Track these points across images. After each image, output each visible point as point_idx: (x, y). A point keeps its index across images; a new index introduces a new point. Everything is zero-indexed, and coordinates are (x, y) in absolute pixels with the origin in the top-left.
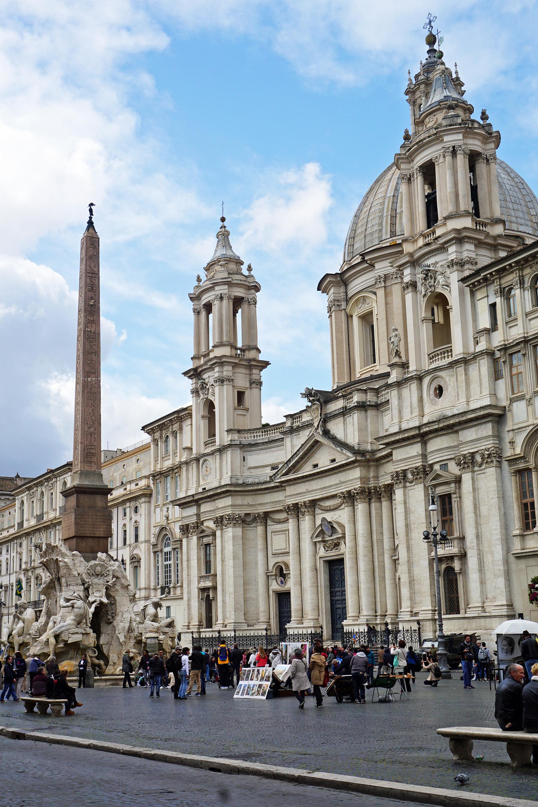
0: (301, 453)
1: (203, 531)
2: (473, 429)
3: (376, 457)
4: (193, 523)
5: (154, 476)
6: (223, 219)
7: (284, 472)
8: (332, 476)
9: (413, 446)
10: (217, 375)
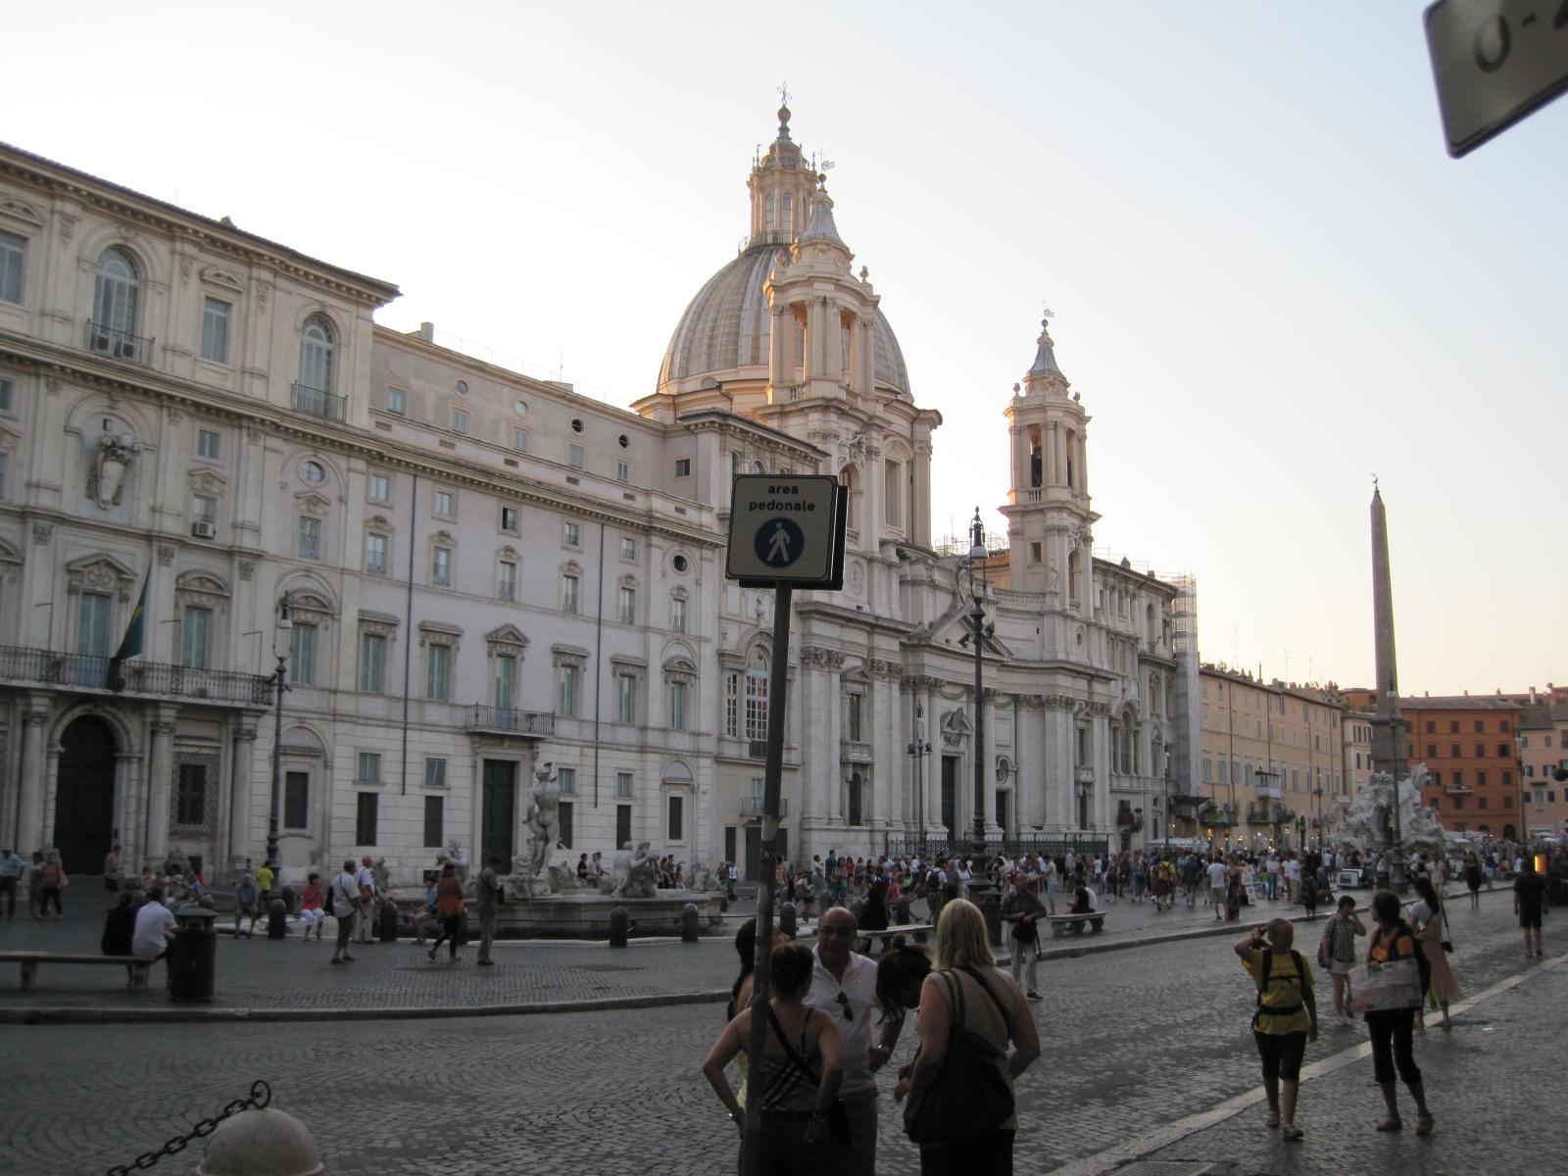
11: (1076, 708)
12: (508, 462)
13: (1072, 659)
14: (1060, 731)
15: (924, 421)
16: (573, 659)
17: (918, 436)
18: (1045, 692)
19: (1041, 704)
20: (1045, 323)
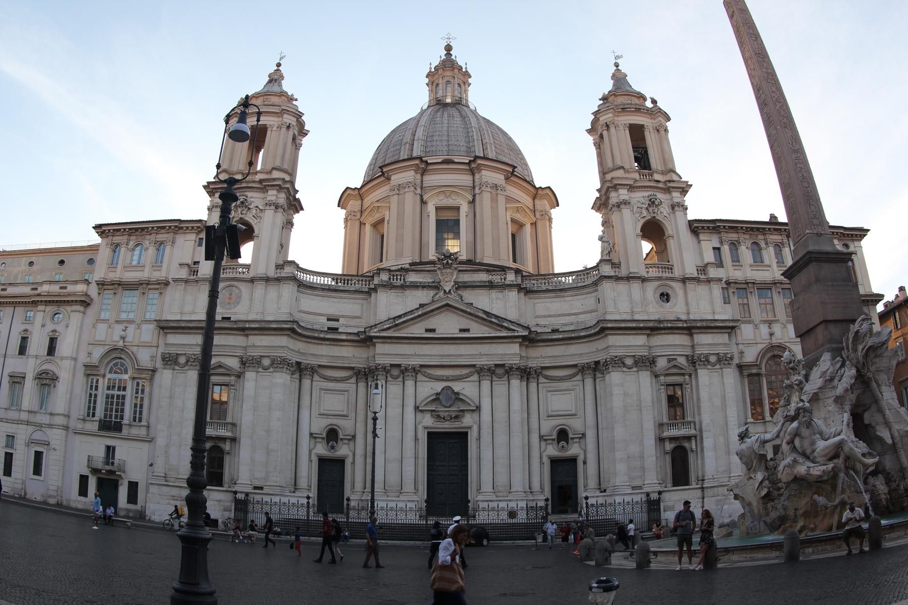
0: (420, 313)
1: (220, 366)
2: (710, 336)
3: (539, 338)
4: (194, 355)
5: (102, 284)
6: (279, 65)
7: (385, 327)
8: (462, 346)
9: (637, 336)
10: (269, 198)
11: (662, 363)
12: (33, 289)
13: (637, 317)
14: (617, 391)
15: (479, 168)
16: (47, 381)
17: (477, 183)
18: (601, 357)
19: (596, 369)
20: (617, 65)
